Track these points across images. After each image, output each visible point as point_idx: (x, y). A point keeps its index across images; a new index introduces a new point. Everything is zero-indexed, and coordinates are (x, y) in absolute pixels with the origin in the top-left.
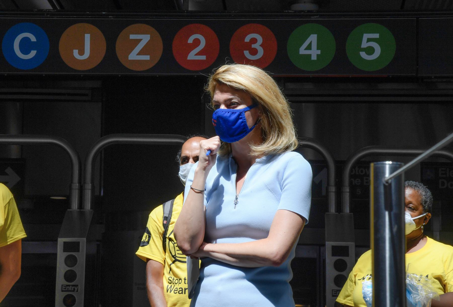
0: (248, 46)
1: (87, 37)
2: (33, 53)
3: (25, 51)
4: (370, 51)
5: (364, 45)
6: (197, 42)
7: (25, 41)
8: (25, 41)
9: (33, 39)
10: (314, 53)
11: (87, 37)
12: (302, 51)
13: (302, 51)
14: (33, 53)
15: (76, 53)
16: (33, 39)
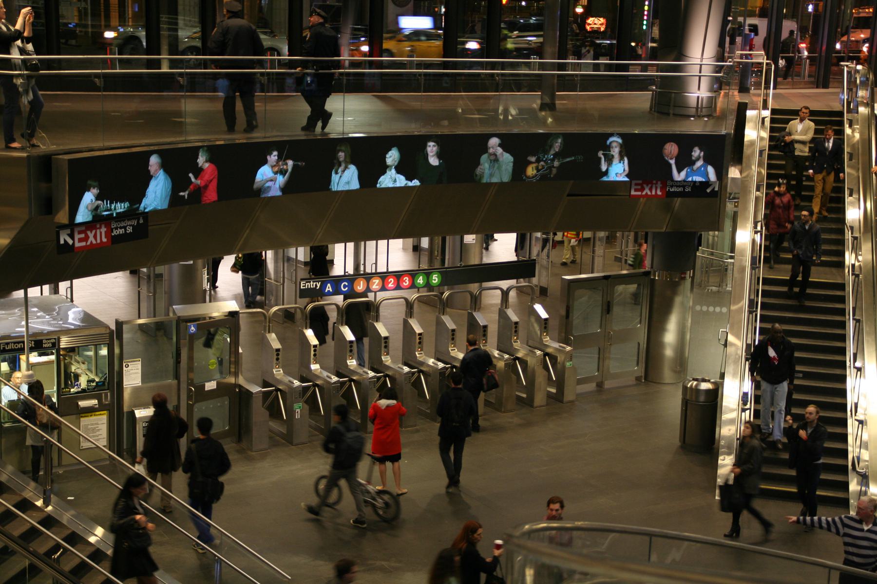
0: (404, 281)
1: (362, 282)
2: (347, 288)
3: (344, 288)
4: (435, 280)
5: (434, 278)
6: (391, 281)
7: (345, 285)
8: (345, 285)
9: (347, 284)
10: (421, 282)
11: (362, 282)
12: (418, 281)
13: (418, 281)
14: (347, 288)
15: (358, 287)
16: (347, 284)
